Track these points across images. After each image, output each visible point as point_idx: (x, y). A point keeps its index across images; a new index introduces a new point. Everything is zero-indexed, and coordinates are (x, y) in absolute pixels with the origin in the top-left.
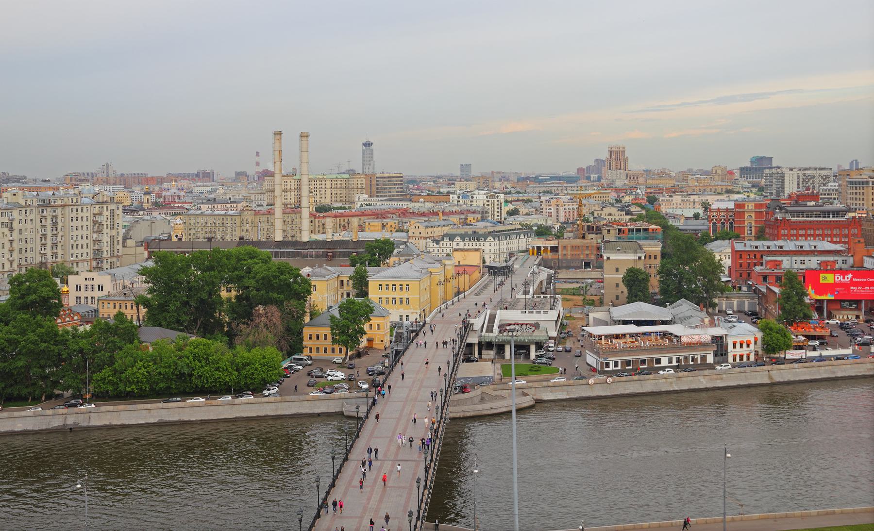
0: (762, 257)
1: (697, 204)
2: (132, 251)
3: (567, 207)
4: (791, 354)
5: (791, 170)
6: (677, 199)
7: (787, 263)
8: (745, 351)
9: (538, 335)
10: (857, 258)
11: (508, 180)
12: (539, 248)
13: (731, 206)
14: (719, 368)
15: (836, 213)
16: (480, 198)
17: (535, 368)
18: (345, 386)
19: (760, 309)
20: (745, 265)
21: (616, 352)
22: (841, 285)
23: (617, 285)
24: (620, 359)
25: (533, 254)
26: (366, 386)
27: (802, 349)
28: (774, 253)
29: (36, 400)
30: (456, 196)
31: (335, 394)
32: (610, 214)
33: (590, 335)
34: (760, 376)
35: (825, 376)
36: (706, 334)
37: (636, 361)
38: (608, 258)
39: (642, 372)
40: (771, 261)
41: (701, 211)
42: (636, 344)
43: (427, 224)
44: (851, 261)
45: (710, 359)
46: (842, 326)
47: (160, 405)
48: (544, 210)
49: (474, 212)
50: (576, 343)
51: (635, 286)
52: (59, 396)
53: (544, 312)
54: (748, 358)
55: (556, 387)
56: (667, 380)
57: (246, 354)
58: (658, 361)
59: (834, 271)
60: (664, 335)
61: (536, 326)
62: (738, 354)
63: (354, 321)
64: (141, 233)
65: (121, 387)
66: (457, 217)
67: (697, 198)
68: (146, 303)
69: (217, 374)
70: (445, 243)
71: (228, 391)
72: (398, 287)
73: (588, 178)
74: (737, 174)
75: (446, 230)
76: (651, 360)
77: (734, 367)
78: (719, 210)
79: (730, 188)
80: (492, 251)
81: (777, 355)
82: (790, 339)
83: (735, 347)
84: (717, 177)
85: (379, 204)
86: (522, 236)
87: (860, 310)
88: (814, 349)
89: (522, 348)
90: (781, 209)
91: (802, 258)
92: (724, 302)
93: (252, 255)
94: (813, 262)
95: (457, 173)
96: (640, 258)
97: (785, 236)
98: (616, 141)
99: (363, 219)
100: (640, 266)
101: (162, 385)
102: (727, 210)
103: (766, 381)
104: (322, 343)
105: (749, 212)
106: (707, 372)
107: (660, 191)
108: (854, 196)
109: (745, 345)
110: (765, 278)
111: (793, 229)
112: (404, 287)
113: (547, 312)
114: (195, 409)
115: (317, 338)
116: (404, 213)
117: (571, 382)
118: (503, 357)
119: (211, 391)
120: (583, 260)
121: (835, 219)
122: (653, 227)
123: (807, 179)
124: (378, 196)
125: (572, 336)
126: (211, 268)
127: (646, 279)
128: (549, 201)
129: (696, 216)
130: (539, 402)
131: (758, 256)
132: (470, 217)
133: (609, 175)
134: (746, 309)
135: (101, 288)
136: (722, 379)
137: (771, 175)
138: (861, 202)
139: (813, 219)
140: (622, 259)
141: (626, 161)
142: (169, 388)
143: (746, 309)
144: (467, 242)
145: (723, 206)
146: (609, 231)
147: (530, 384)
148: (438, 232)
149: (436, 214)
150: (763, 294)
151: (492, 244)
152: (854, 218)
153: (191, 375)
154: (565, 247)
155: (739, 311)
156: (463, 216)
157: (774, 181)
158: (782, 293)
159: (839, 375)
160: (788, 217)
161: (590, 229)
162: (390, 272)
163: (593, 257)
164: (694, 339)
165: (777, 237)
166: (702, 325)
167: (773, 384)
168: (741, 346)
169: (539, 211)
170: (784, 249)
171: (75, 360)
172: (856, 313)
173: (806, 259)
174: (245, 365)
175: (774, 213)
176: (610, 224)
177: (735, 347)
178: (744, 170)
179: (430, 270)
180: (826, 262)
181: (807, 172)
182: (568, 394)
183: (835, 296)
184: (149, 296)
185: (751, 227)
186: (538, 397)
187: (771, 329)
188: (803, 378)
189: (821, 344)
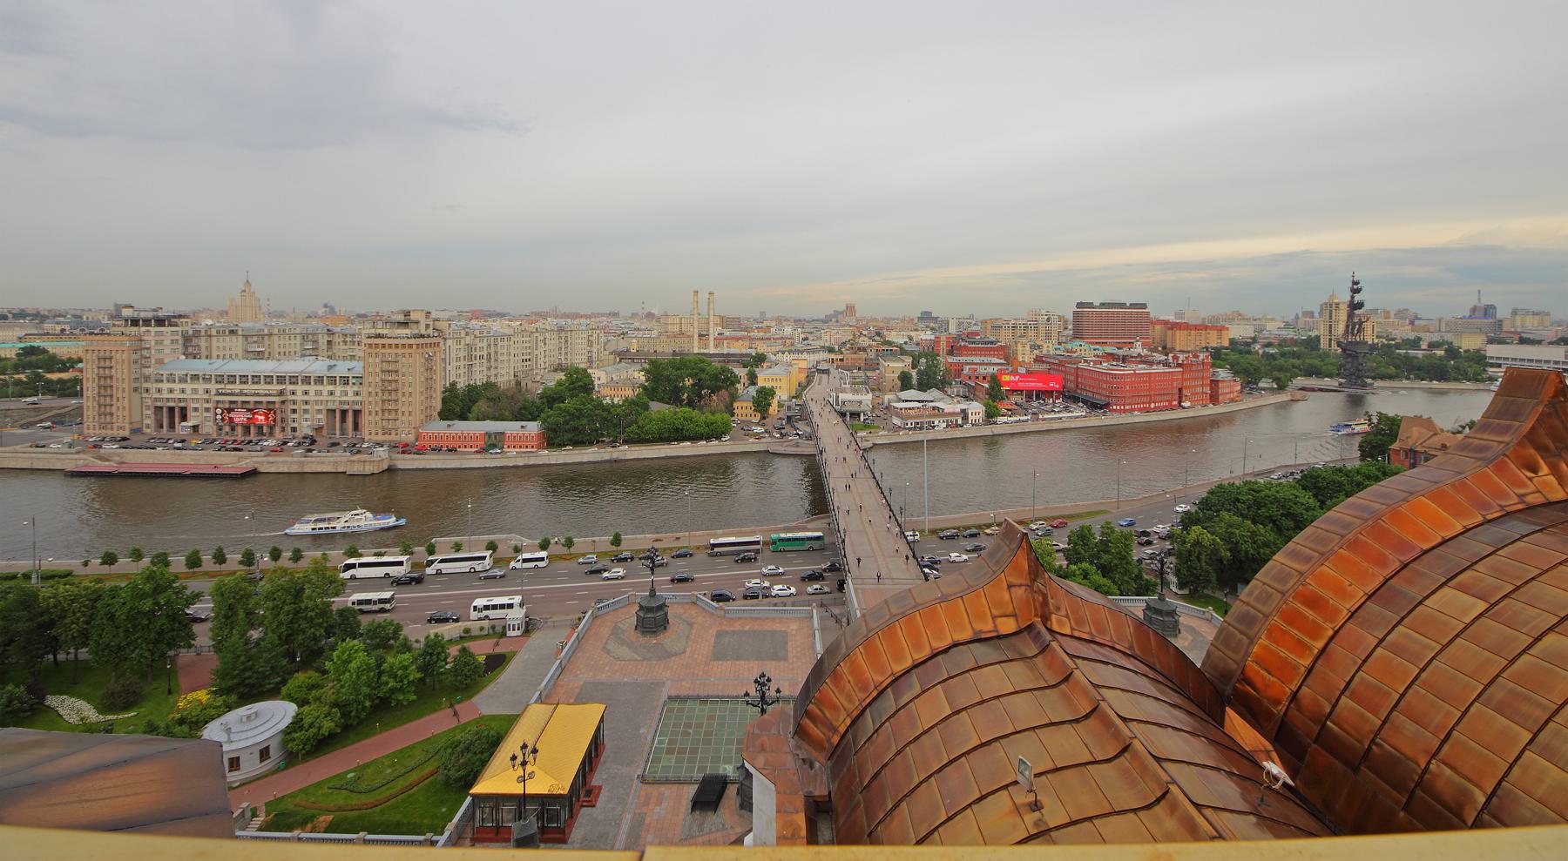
7: (982, 370)
9: (863, 408)
16: (788, 330)
17: (866, 426)
21: (911, 417)
29: (591, 444)
34: (987, 431)
36: (958, 408)
51: (905, 382)
55: (882, 437)
68: (645, 388)
80: (806, 361)
89: (855, 415)
93: (702, 361)
94: (991, 370)
95: (757, 316)
114: (685, 449)
115: (744, 409)
116: (751, 339)
119: (694, 438)
123: (960, 324)
169: (820, 338)
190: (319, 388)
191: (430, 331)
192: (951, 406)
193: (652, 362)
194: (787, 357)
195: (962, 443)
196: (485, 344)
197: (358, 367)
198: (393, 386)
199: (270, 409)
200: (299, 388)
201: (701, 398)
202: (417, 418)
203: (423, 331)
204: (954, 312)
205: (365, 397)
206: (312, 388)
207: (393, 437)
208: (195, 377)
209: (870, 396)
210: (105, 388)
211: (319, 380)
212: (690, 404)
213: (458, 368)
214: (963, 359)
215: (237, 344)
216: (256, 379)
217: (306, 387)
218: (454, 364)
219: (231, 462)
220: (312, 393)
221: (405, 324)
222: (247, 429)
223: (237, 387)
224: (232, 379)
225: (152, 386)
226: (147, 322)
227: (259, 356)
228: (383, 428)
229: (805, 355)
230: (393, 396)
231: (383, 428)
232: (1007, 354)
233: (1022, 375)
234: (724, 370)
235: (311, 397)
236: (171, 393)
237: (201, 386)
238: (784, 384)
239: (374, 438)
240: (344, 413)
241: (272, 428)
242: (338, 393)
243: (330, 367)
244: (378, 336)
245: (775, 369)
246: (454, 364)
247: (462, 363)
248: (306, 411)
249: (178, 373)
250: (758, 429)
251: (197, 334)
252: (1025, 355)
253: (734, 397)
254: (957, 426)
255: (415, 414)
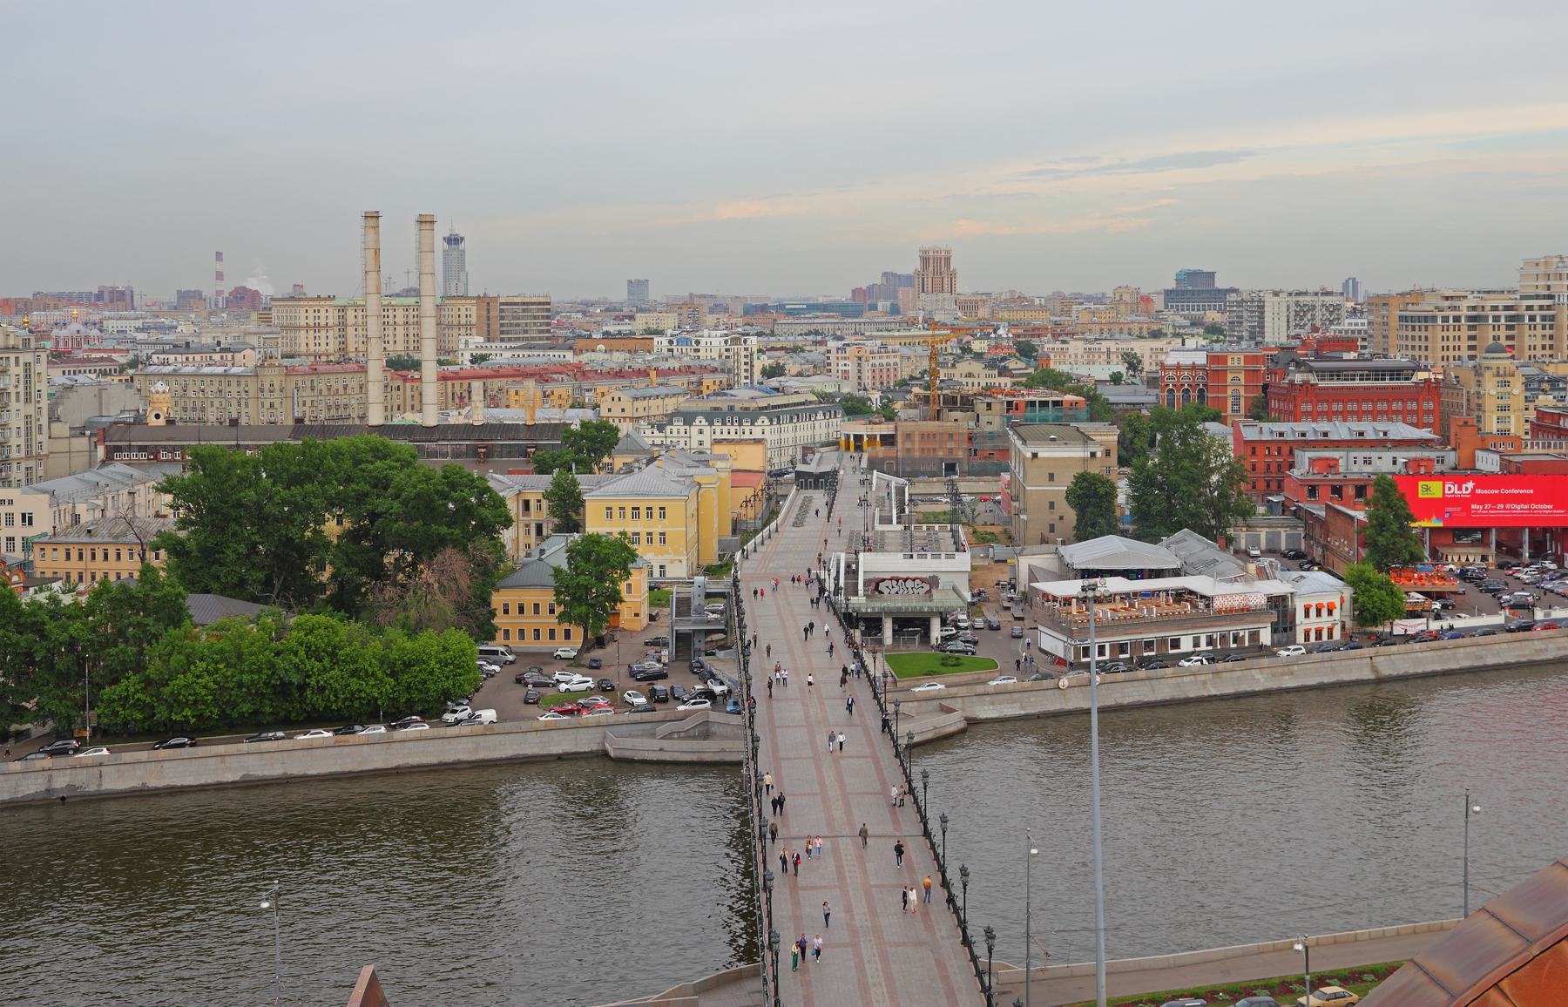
0: (1291, 452)
1: (1113, 357)
2: (62, 445)
3: (877, 362)
4: (1401, 626)
5: (1276, 294)
6: (1076, 346)
7: (1352, 465)
8: (1325, 621)
9: (941, 599)
10: (1465, 452)
11: (726, 310)
12: (858, 438)
13: (1201, 359)
14: (1283, 653)
15: (1396, 373)
16: (712, 344)
17: (949, 661)
18: (601, 702)
19: (1309, 546)
20: (1261, 467)
22: (1455, 501)
23: (1052, 505)
24: (1107, 641)
25: (848, 448)
26: (642, 700)
27: (1420, 616)
28: (1314, 445)
30: (664, 340)
31: (586, 716)
32: (970, 375)
33: (1045, 595)
34: (1357, 666)
35: (1467, 664)
36: (1259, 592)
37: (1135, 644)
38: (1035, 455)
39: (1144, 663)
40: (1320, 459)
41: (1122, 368)
42: (1134, 612)
43: (633, 392)
44: (1451, 458)
45: (1266, 637)
46: (1463, 575)
47: (245, 746)
48: (833, 367)
49: (715, 371)
50: (1003, 613)
51: (1091, 508)
52: (21, 735)
53: (948, 557)
54: (1330, 636)
55: (1000, 695)
56: (1192, 680)
57: (409, 645)
58: (1176, 643)
59: (1442, 476)
60: (1180, 595)
61: (933, 582)
62: (1313, 627)
63: (601, 579)
64: (79, 410)
65: (162, 713)
66: (684, 379)
67: (1113, 346)
68: (178, 550)
69: (354, 684)
70: (675, 429)
71: (372, 718)
72: (643, 512)
73: (873, 307)
74: (1159, 303)
75: (670, 405)
76: (1163, 641)
77: (1309, 652)
78: (1178, 367)
79: (1155, 327)
80: (774, 442)
81: (1380, 629)
82: (1401, 600)
83: (1307, 615)
84: (1122, 308)
85: (503, 355)
86: (820, 415)
87: (1487, 545)
88: (1438, 617)
89: (912, 625)
90: (1298, 364)
91: (1367, 454)
92: (1243, 535)
93: (380, 453)
94: (1385, 463)
95: (619, 295)
96: (1093, 455)
97: (1307, 414)
98: (934, 237)
99: (496, 384)
100: (1094, 469)
101: (246, 708)
102: (1194, 367)
103: (1368, 675)
104: (529, 621)
105: (1236, 370)
106: (1265, 661)
107: (1038, 332)
108: (1410, 343)
109: (1324, 612)
110: (1313, 491)
111: (1322, 401)
112: (656, 512)
113: (952, 556)
114: (314, 752)
115: (526, 612)
116: (580, 372)
117: (1027, 684)
118: (880, 642)
119: (344, 719)
120: (942, 460)
121: (1395, 383)
122: (1069, 397)
123: (1301, 312)
124: (502, 340)
125: (986, 600)
126: (297, 480)
127: (1111, 493)
128: (842, 349)
129: (1116, 379)
130: (973, 722)
131: (1285, 450)
132: (708, 380)
133: (919, 305)
134: (1283, 547)
135: (27, 519)
136: (1292, 673)
137: (1240, 304)
138: (1423, 353)
139: (1357, 383)
140: (1055, 459)
141: (953, 276)
142: (256, 713)
143: (1283, 547)
144: (718, 427)
145: (1186, 359)
146: (989, 405)
147: (953, 690)
148: (657, 408)
149: (643, 373)
150: (1317, 519)
151: (767, 430)
152: (1427, 381)
153: (302, 687)
154: (908, 436)
155: (1271, 552)
156: (694, 378)
157: (1245, 314)
158: (1370, 517)
159: (1491, 661)
160: (1313, 379)
161: (951, 402)
162: (625, 483)
163: (960, 454)
164: (1237, 603)
165: (1296, 417)
166: (1246, 579)
167: (1380, 681)
168: (1319, 614)
169: (823, 367)
170: (1332, 437)
171: (61, 664)
172: (1481, 550)
173: (1374, 455)
174: (408, 665)
175: (1285, 373)
176: (989, 391)
177: (1307, 615)
178: (1170, 295)
179: (697, 479)
180: (1417, 462)
181: (1301, 299)
182: (1022, 708)
183: (1445, 521)
184: (182, 534)
185: (1237, 398)
186: (969, 715)
187: (1368, 582)
188: (1429, 668)
189: (1444, 607)
192: (1230, 587)
193: (201, 460)
194: (700, 434)
195: (1276, 712)
201: (377, 572)
204: (1282, 267)
209: (963, 561)
212: (346, 602)
214: (1290, 429)
229: (761, 428)
232: (1443, 408)
233: (1484, 479)
234: (453, 482)
238: (677, 526)
245: (648, 476)
250: (576, 681)
252: (1506, 409)
253: (489, 573)
254: (1261, 651)
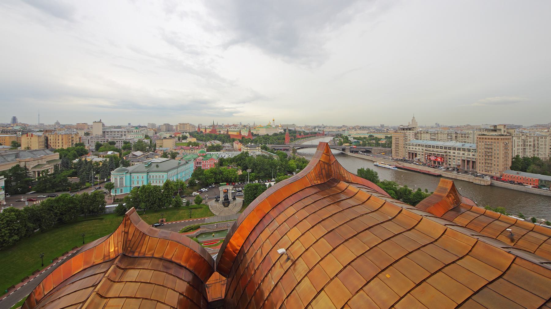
190: (459, 152)
191: (505, 133)
196: (532, 140)
197: (474, 146)
198: (490, 154)
199: (442, 157)
200: (452, 151)
202: (501, 168)
203: (503, 133)
205: (478, 157)
206: (456, 152)
207: (489, 173)
208: (419, 145)
210: (397, 146)
211: (459, 149)
213: (518, 149)
215: (428, 136)
216: (437, 147)
217: (454, 151)
218: (516, 147)
219: (432, 170)
220: (456, 153)
221: (495, 131)
222: (435, 162)
223: (431, 149)
224: (430, 146)
225: (408, 147)
226: (407, 129)
227: (434, 140)
228: (485, 169)
230: (490, 158)
231: (485, 169)
235: (456, 154)
236: (413, 149)
237: (421, 148)
239: (481, 172)
240: (468, 161)
241: (442, 163)
242: (466, 154)
243: (463, 145)
244: (484, 135)
246: (516, 147)
247: (520, 147)
248: (454, 159)
249: (415, 143)
251: (418, 133)
255: (500, 166)
